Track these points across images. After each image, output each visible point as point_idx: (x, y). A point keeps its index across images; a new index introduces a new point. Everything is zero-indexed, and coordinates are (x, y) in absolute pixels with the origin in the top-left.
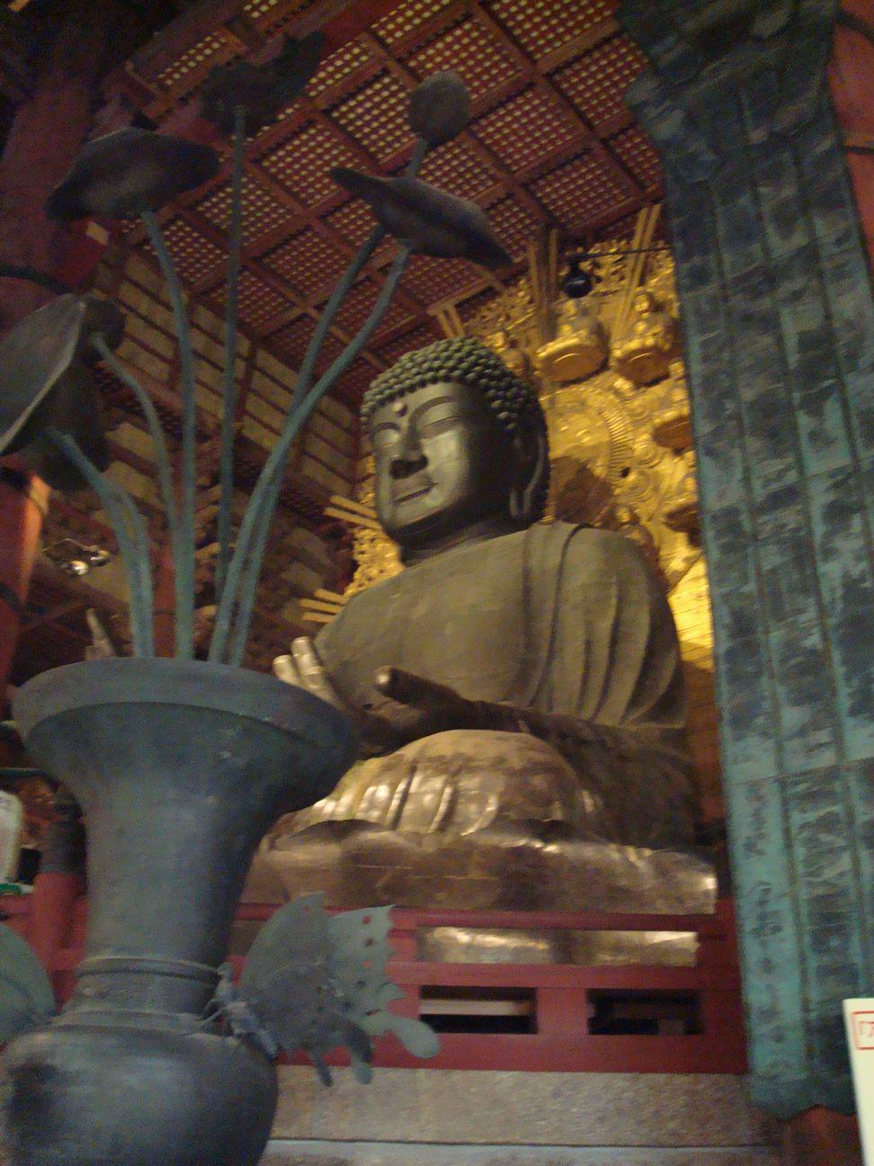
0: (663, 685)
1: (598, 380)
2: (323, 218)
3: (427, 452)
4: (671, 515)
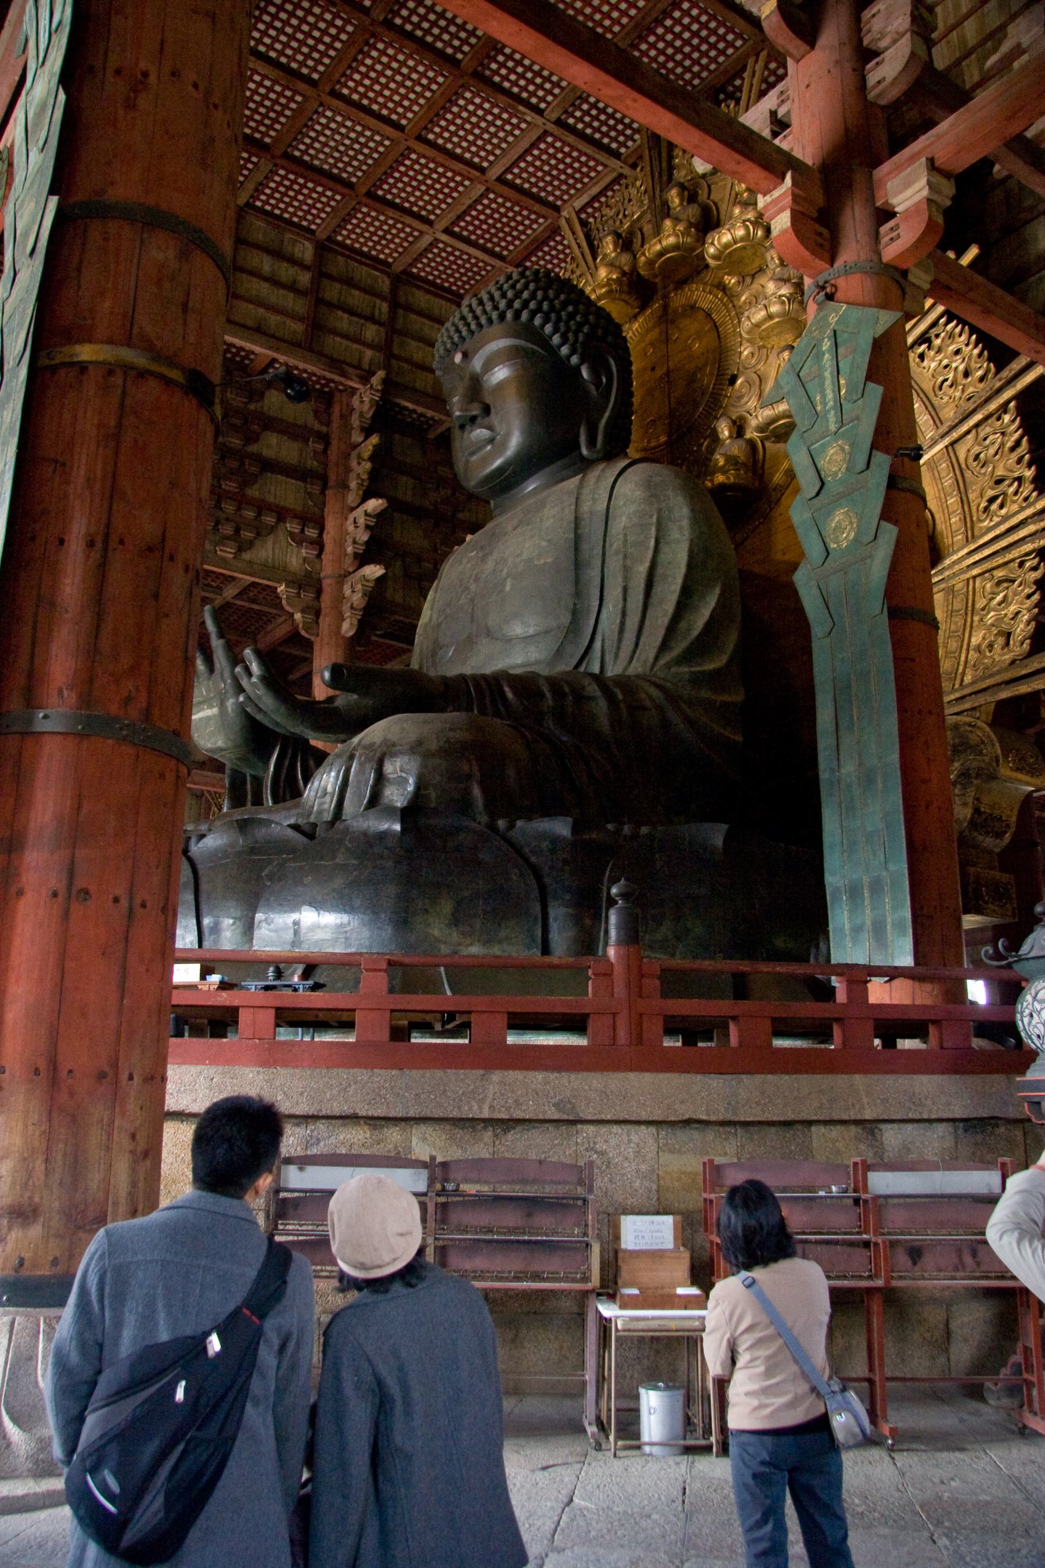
1: (708, 277)
2: (421, 139)
3: (488, 400)
4: (761, 429)
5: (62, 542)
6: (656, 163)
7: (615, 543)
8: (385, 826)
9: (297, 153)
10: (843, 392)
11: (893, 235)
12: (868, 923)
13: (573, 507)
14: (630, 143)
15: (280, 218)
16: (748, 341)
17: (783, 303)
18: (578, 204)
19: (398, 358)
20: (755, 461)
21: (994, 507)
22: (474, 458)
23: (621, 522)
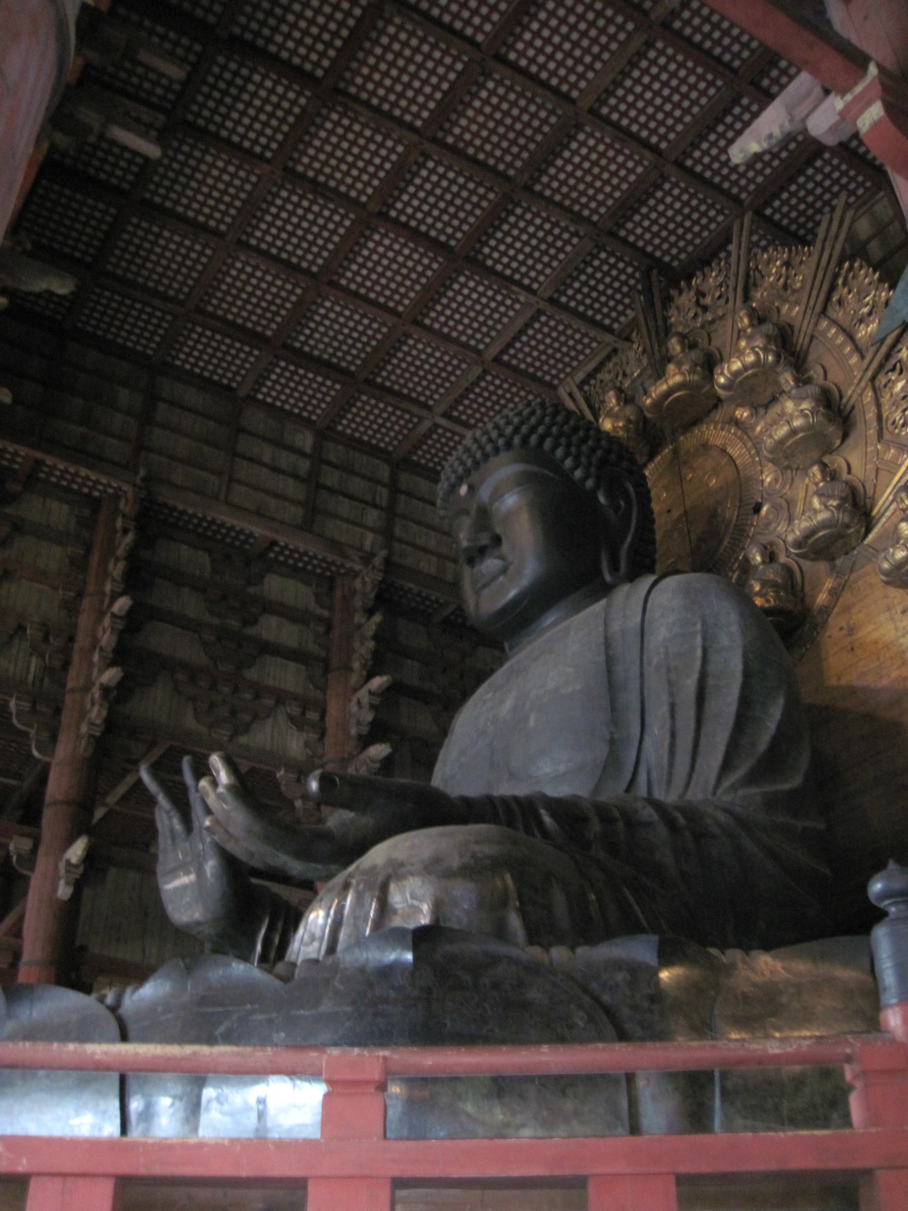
0: (763, 742)
1: (718, 415)
2: (417, 323)
3: (498, 531)
4: (798, 544)
6: (651, 324)
7: (655, 658)
8: (392, 956)
9: (297, 345)
13: (601, 629)
14: (622, 319)
15: (281, 409)
16: (772, 461)
17: (806, 416)
19: (400, 541)
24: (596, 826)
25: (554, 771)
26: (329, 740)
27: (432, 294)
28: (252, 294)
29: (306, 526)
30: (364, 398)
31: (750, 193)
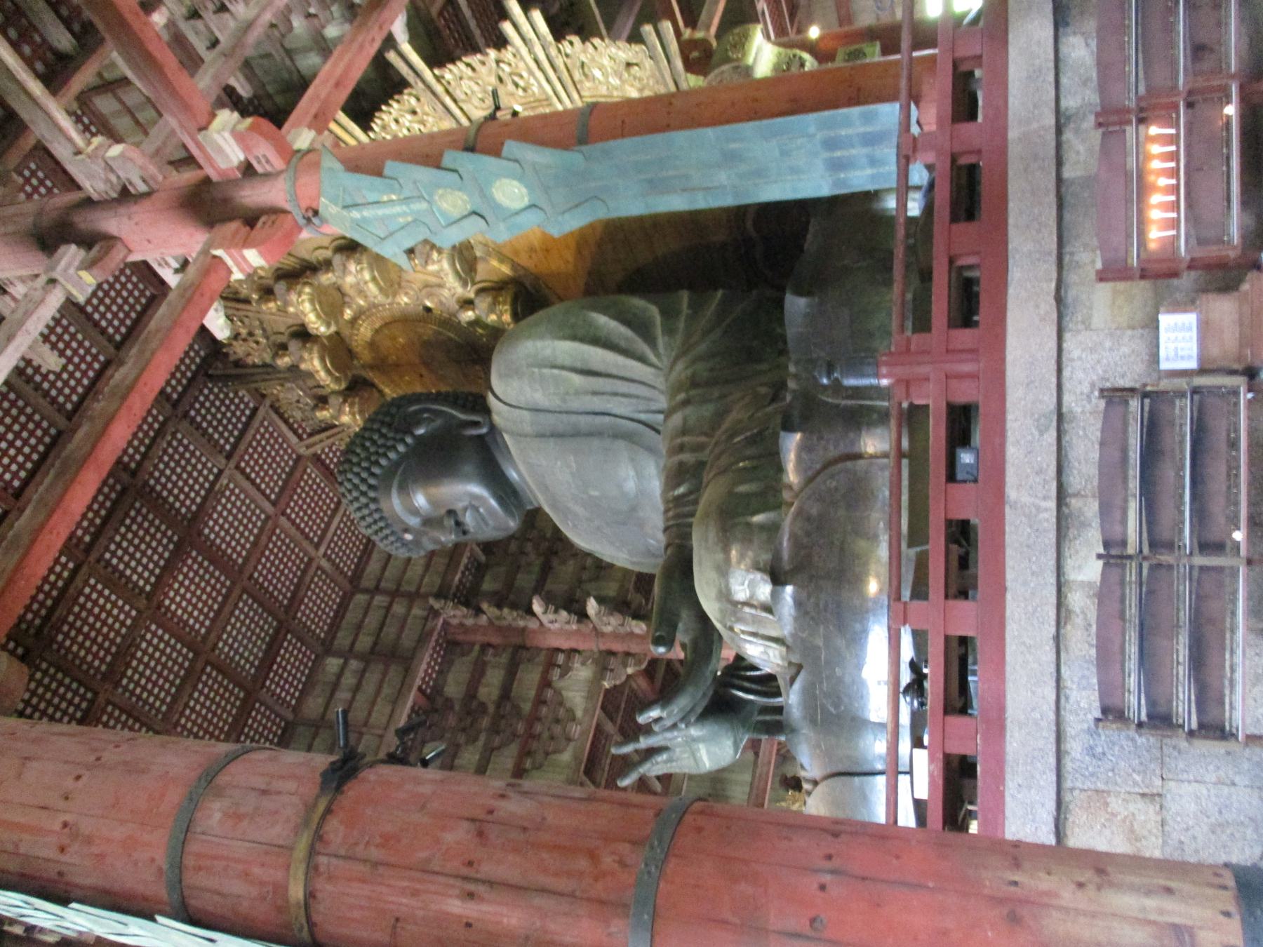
1: (346, 332)
3: (443, 511)
4: (465, 284)
5: (469, 925)
7: (555, 403)
10: (394, 197)
11: (263, 161)
12: (865, 151)
14: (246, 400)
18: (294, 439)
20: (493, 289)
21: (521, 83)
22: (491, 522)
23: (539, 397)
24: (687, 457)
25: (641, 480)
26: (581, 647)
27: (216, 558)
28: (209, 709)
29: (407, 662)
30: (299, 615)
31: (146, 288)
